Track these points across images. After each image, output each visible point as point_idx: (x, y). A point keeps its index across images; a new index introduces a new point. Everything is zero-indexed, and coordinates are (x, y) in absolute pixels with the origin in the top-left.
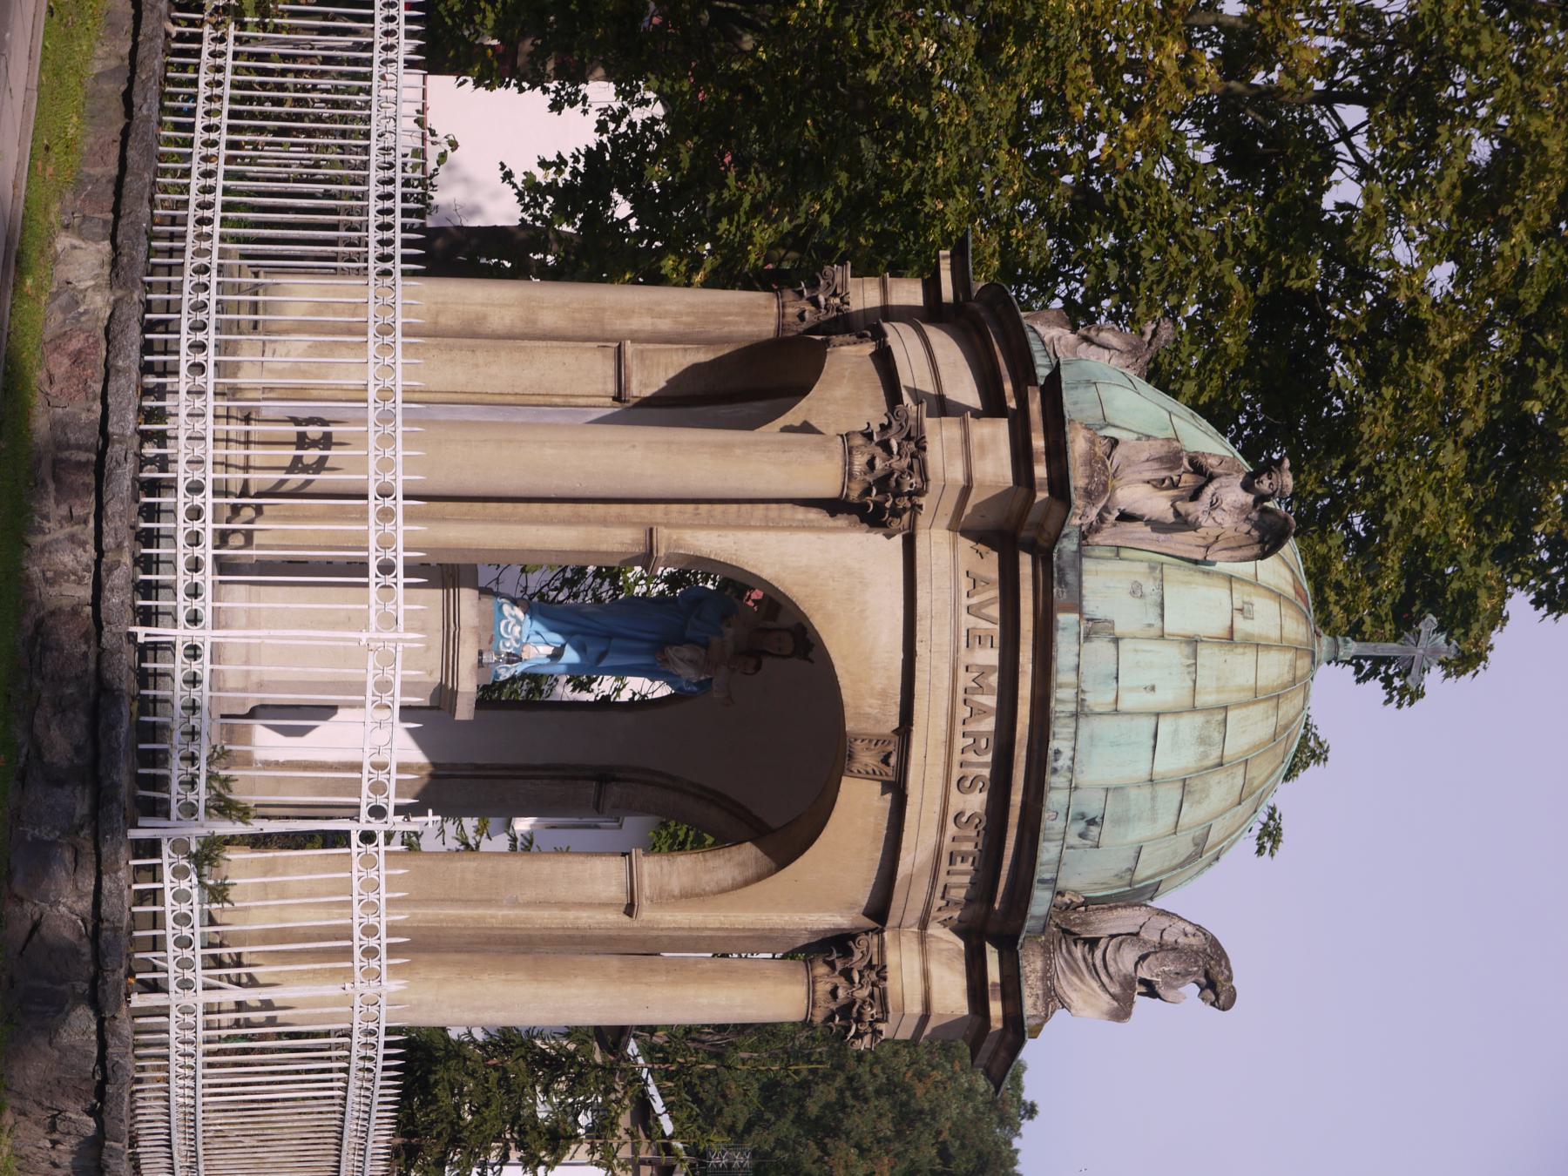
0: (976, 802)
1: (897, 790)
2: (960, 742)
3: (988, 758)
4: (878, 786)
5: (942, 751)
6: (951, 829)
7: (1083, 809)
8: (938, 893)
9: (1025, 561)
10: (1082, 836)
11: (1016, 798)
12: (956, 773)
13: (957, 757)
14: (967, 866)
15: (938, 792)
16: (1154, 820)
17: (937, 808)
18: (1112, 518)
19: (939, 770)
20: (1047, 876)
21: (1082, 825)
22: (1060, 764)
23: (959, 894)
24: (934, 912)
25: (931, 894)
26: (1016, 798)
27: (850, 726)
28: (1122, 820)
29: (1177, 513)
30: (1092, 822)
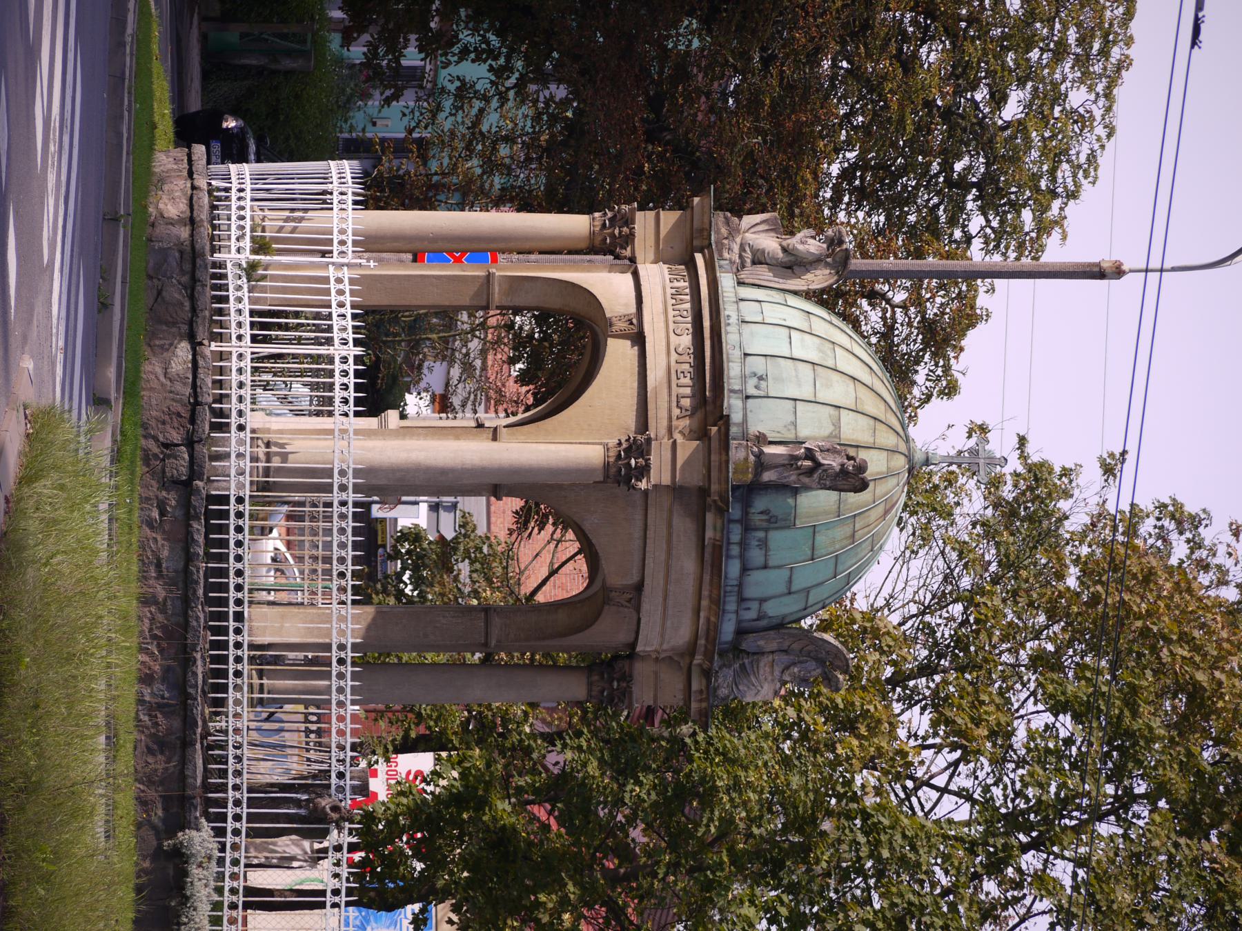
0: (686, 340)
1: (639, 339)
2: (671, 313)
3: (689, 319)
4: (628, 343)
5: (662, 318)
6: (674, 356)
7: (754, 370)
8: (674, 404)
9: (699, 258)
10: (757, 387)
11: (707, 323)
12: (672, 326)
13: (671, 319)
14: (687, 381)
15: (663, 335)
16: (800, 385)
17: (664, 343)
18: (749, 261)
19: (662, 325)
20: (737, 387)
21: (753, 381)
22: (731, 321)
23: (686, 402)
24: (675, 423)
25: (670, 402)
26: (707, 323)
27: (608, 315)
28: (779, 380)
29: (785, 250)
30: (761, 378)
